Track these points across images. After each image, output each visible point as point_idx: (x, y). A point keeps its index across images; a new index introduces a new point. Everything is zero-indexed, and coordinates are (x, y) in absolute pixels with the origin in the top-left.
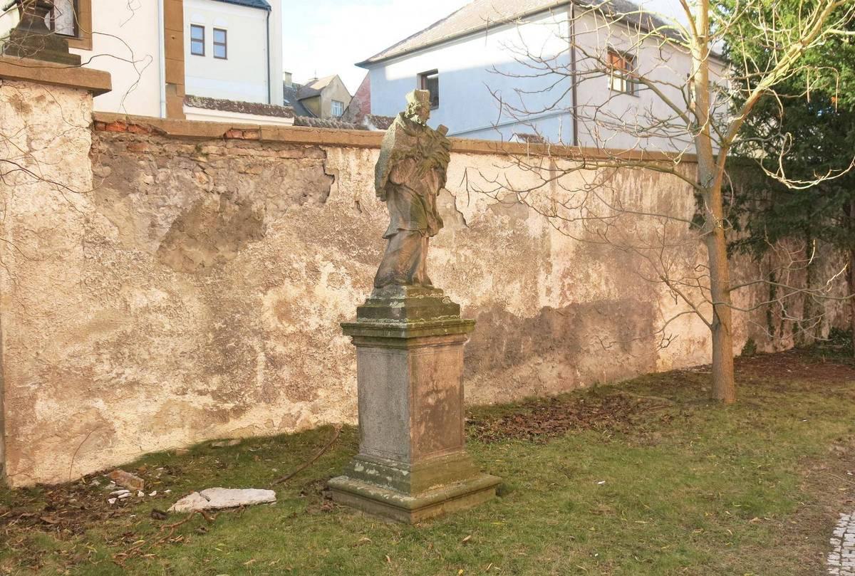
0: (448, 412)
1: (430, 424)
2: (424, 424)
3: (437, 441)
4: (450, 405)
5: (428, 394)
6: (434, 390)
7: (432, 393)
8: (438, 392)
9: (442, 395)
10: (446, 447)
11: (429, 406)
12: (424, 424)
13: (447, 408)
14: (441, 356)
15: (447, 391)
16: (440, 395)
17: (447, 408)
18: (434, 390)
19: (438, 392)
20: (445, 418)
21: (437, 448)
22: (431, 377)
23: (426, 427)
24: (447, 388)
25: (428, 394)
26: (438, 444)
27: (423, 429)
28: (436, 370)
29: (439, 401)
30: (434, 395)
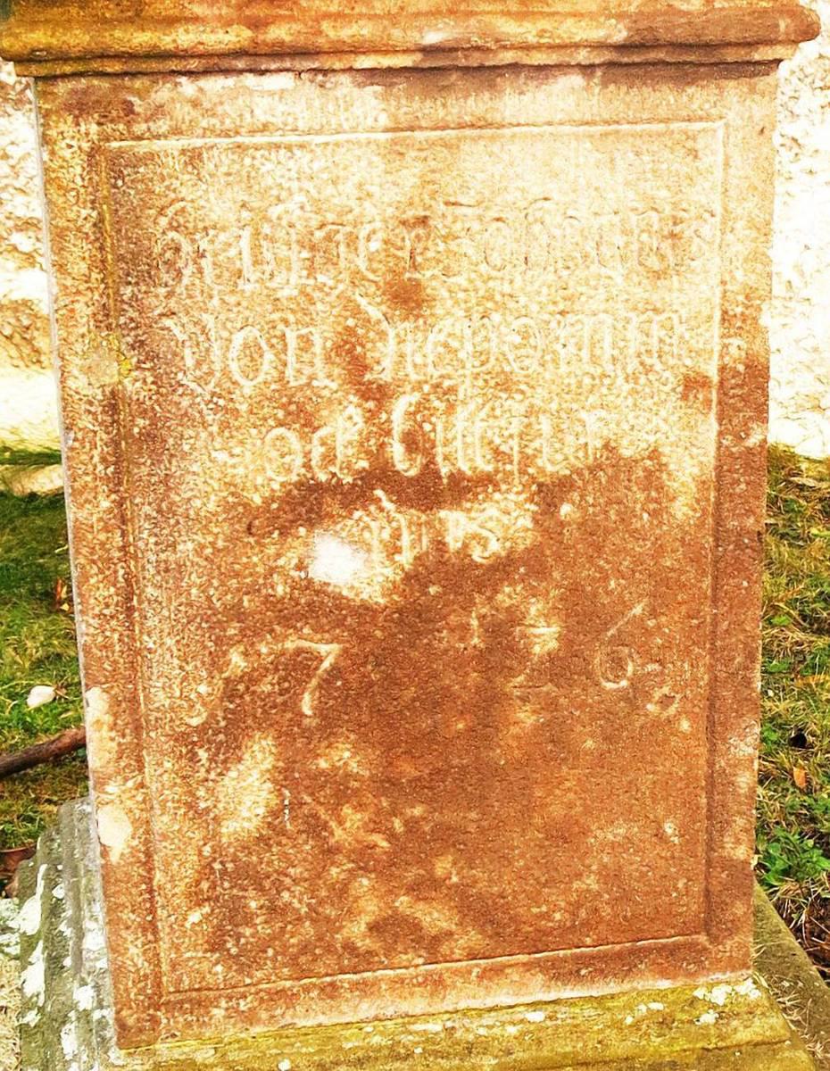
0: (562, 667)
1: (343, 756)
2: (260, 755)
3: (425, 888)
4: (583, 615)
5: (309, 504)
6: (380, 475)
7: (356, 494)
8: (430, 491)
9: (487, 527)
10: (506, 934)
11: (318, 607)
12: (260, 755)
13: (544, 636)
14: (478, 165)
15: (549, 494)
16: (457, 525)
17: (544, 636)
18: (380, 475)
19: (430, 491)
20: (526, 717)
21: (432, 946)
22: (351, 357)
23: (285, 776)
24: (551, 464)
25: (309, 504)
26: (435, 917)
27: (247, 791)
28: (407, 298)
29: (444, 580)
30: (386, 519)
